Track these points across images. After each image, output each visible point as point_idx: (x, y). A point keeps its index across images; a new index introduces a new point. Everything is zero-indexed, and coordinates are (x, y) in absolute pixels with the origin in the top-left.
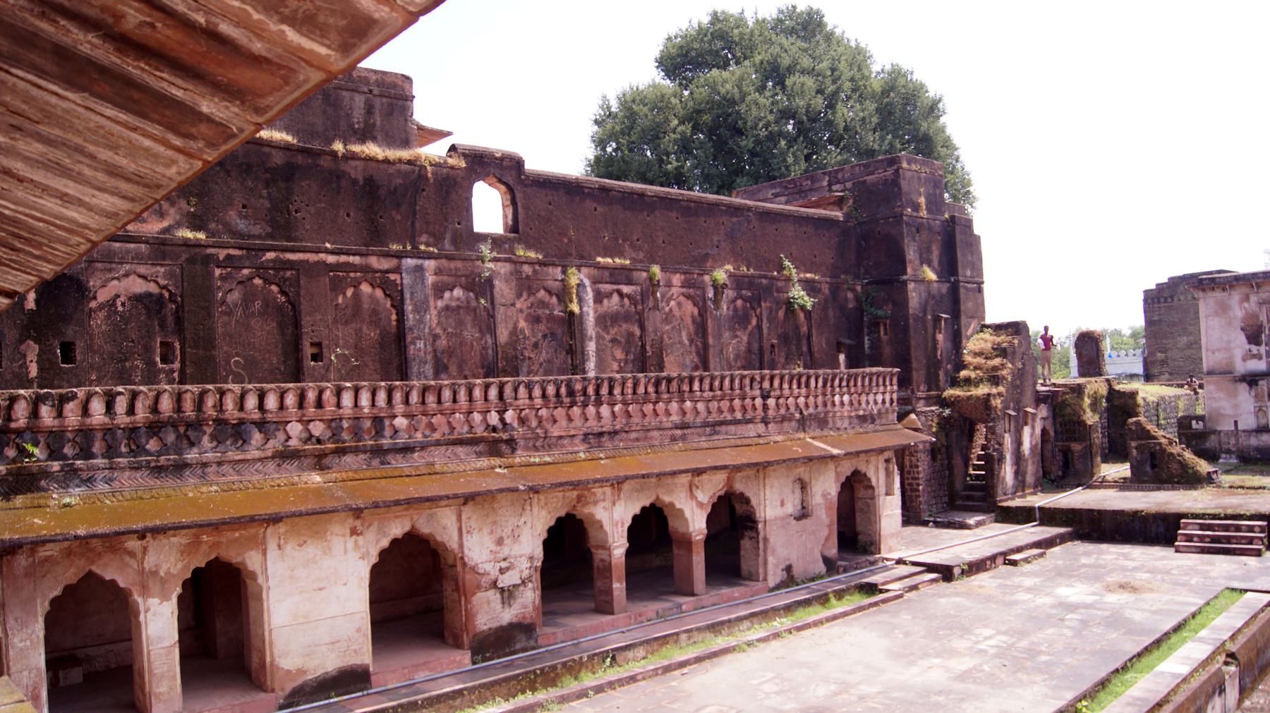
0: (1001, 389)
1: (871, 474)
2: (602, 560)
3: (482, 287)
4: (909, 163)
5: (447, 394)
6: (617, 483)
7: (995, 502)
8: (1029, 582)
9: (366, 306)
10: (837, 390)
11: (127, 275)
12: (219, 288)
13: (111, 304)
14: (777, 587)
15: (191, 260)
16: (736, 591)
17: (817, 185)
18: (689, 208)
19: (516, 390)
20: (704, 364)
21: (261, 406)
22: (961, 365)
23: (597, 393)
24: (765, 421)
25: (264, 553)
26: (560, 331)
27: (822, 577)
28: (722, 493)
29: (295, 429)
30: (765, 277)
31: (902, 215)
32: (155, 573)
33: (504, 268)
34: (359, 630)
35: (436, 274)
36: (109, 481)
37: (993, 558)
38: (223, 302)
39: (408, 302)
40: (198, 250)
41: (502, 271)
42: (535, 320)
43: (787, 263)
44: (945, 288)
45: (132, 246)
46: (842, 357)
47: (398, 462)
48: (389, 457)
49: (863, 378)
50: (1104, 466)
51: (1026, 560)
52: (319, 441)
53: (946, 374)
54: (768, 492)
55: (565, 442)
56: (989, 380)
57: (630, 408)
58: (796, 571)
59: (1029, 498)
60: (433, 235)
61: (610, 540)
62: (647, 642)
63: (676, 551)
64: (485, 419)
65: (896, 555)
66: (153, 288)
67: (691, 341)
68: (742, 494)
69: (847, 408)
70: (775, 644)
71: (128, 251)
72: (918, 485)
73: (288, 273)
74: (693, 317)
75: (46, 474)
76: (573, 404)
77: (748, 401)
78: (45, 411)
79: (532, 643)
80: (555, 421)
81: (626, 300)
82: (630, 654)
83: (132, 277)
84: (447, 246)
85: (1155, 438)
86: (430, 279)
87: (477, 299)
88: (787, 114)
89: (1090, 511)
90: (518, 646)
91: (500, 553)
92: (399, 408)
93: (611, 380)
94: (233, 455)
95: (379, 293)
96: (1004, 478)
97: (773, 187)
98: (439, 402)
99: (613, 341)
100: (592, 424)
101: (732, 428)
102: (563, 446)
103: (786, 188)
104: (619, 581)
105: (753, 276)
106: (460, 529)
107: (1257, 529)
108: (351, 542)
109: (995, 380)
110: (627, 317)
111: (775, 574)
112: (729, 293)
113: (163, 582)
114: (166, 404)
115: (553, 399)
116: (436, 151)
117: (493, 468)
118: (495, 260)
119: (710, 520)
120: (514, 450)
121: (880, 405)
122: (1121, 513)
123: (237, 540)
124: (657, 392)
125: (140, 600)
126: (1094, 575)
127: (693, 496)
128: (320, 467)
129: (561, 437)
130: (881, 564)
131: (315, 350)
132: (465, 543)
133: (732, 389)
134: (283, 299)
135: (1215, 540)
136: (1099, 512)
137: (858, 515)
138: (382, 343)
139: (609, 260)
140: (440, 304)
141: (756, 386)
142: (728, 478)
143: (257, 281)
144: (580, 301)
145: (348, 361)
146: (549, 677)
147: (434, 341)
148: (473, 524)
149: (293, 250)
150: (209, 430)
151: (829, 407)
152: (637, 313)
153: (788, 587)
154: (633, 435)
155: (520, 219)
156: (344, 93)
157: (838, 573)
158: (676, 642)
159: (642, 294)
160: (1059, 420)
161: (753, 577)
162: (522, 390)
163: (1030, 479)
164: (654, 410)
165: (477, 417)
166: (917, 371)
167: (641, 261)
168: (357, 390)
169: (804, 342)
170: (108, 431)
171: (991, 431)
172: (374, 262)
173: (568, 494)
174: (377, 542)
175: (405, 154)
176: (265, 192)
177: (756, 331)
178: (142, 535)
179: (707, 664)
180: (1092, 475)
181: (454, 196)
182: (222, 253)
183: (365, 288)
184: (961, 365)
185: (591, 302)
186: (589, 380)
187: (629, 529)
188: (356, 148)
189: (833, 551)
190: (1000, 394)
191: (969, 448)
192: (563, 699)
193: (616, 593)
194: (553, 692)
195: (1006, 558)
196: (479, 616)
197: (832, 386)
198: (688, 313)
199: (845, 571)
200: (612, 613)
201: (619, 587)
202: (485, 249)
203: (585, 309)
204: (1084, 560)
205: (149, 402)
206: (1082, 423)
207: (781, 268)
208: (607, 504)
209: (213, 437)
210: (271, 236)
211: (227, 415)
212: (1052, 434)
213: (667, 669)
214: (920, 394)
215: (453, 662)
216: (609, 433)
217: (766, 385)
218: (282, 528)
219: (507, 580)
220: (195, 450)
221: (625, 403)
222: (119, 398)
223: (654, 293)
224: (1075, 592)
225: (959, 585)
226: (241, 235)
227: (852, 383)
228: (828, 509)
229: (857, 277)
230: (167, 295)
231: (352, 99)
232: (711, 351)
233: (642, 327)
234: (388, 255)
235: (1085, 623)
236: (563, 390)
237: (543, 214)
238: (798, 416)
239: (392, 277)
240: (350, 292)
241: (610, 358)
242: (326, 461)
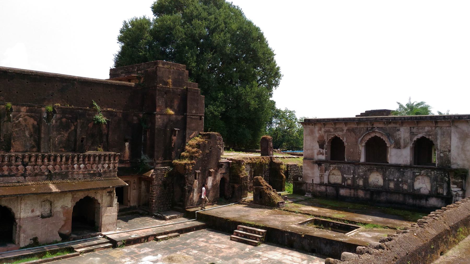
1: (98, 197)
4: (164, 64)
17: (133, 70)
20: (38, 146)
22: (183, 150)
24: (24, 175)
30: (81, 109)
31: (156, 86)
44: (180, 118)
46: (127, 144)
54: (23, 206)
58: (40, 240)
59: (207, 208)
67: (31, 136)
72: (153, 199)
74: (34, 126)
85: (262, 186)
88: (192, 37)
96: (192, 199)
103: (125, 70)
107: (261, 233)
109: (191, 158)
111: (25, 241)
121: (106, 169)
135: (245, 236)
151: (70, 170)
153: (34, 247)
157: (70, 241)
180: (241, 198)
189: (67, 231)
190: (192, 164)
197: (73, 161)
212: (228, 179)
217: (26, 160)
223: (8, 115)
227: (87, 159)
232: (42, 140)
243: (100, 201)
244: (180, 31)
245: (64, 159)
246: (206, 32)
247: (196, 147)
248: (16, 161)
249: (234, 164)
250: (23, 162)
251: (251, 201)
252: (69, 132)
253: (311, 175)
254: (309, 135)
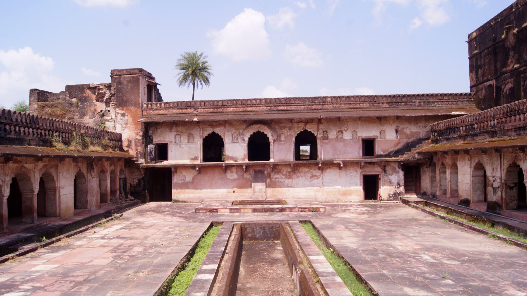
11: (508, 83)
13: (506, 92)
47: (475, 138)
100: (518, 124)
128: (464, 140)
129: (508, 130)
219: (496, 185)
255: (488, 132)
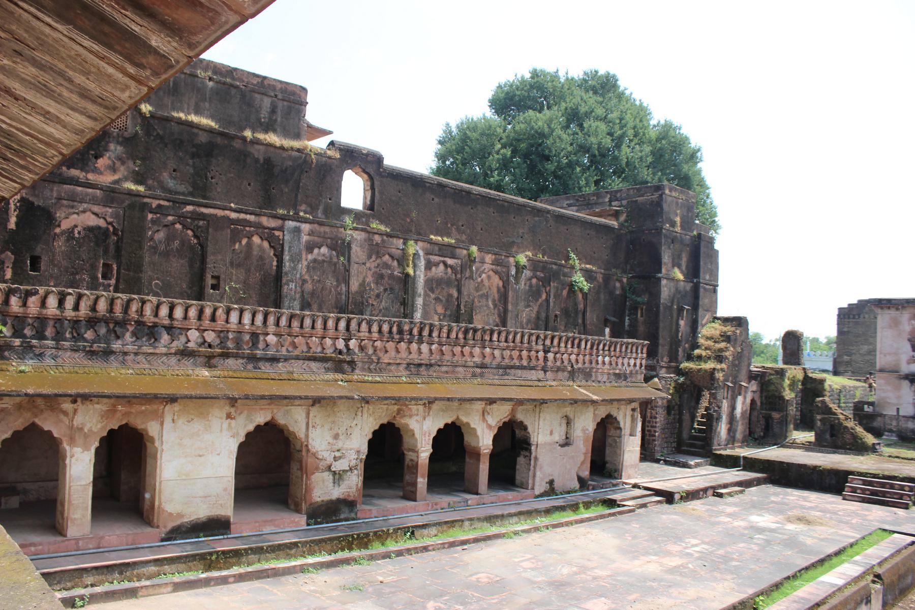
0: (724, 366)
1: (620, 418)
2: (412, 460)
3: (342, 247)
4: (670, 191)
5: (308, 322)
6: (430, 403)
7: (711, 450)
8: (729, 510)
9: (255, 253)
10: (601, 352)
11: (84, 212)
12: (150, 228)
14: (541, 495)
15: (132, 206)
16: (510, 495)
18: (503, 206)
19: (359, 325)
20: (504, 323)
21: (171, 315)
22: (695, 346)
23: (420, 334)
25: (162, 424)
26: (397, 287)
27: (575, 492)
28: (507, 420)
29: (194, 335)
31: (662, 228)
32: (81, 429)
33: (359, 236)
34: (225, 490)
35: (309, 235)
36: (54, 358)
37: (705, 490)
38: (152, 239)
39: (286, 253)
40: (137, 199)
41: (359, 238)
42: (379, 278)
43: (572, 255)
44: (689, 286)
45: (90, 190)
46: (607, 330)
47: (266, 368)
48: (261, 364)
49: (621, 345)
50: (795, 433)
51: (730, 494)
52: (210, 346)
53: (684, 351)
55: (393, 368)
56: (715, 359)
57: (444, 348)
58: (556, 485)
59: (737, 450)
60: (310, 206)
61: (419, 445)
62: (439, 524)
63: (467, 460)
64: (334, 344)
65: (633, 481)
66: (102, 223)
67: (495, 306)
68: (521, 422)
69: (607, 366)
70: (535, 535)
71: (87, 194)
72: (655, 432)
73: (201, 223)
74: (498, 288)
75: (9, 347)
76: (401, 340)
77: (533, 353)
78: (14, 301)
79: (353, 515)
80: (386, 352)
81: (449, 270)
82: (425, 531)
83: (88, 213)
84: (320, 215)
85: (835, 414)
86: (305, 238)
87: (338, 256)
88: (584, 149)
89: (782, 463)
90: (342, 516)
91: (336, 447)
92: (271, 328)
93: (431, 325)
94: (146, 349)
95: (266, 244)
96: (719, 433)
97: (568, 199)
98: (301, 327)
99: (437, 299)
101: (519, 371)
102: (390, 371)
103: (577, 200)
104: (423, 477)
105: (546, 262)
106: (308, 424)
108: (226, 423)
109: (720, 359)
110: (449, 283)
111: (540, 485)
112: (527, 273)
113: (86, 436)
114: (102, 306)
115: (387, 335)
116: (320, 144)
117: (336, 381)
118: (355, 229)
119: (496, 439)
120: (353, 370)
121: (632, 368)
122: (805, 466)
123: (142, 412)
124: (465, 338)
125: (68, 448)
126: (778, 510)
127: (484, 420)
128: (210, 366)
129: (389, 364)
130: (621, 487)
131: (214, 282)
132: (310, 434)
133: (522, 342)
134: (195, 241)
136: (788, 464)
137: (607, 448)
138: (263, 283)
139: (440, 238)
140: (310, 257)
141: (540, 342)
142: (513, 410)
143: (178, 226)
144: (415, 266)
145: (238, 292)
146: (363, 541)
147: (303, 284)
148: (318, 421)
149: (206, 206)
150: (131, 329)
151: (594, 365)
152: (457, 280)
154: (444, 369)
155: (376, 201)
156: (256, 95)
157: (588, 490)
158: (461, 526)
159: (462, 266)
160: (764, 394)
161: (524, 486)
162: (364, 325)
163: (739, 436)
164: (462, 352)
165: (328, 342)
166: (663, 346)
167: (463, 242)
168: (242, 312)
169: (580, 316)
170: (58, 321)
171: (714, 396)
172: (265, 221)
173: (390, 407)
174: (245, 426)
175: (296, 144)
176: (191, 162)
177: (545, 304)
178: (74, 399)
179: (482, 544)
180: (786, 437)
181: (328, 179)
182: (155, 203)
183: (256, 240)
184: (695, 346)
185: (423, 268)
186: (415, 324)
187: (434, 439)
188: (261, 136)
189: (586, 473)
190: (722, 370)
191: (696, 408)
192: (372, 558)
193: (419, 486)
194: (364, 552)
195: (715, 491)
196: (315, 490)
197: (597, 349)
198: (495, 284)
199: (593, 489)
200: (415, 500)
201: (422, 482)
202: (348, 220)
203: (418, 273)
204: (773, 498)
205: (90, 303)
206: (781, 398)
207: (568, 258)
208: (419, 418)
209: (134, 334)
210: (191, 194)
211: (145, 319)
212: (759, 403)
213: (452, 545)
214: (663, 364)
215: (293, 522)
216: (426, 365)
217: (548, 342)
218: (176, 407)
219: (338, 466)
220: (120, 342)
221: (440, 344)
222: (68, 298)
223: (471, 267)
224: (764, 520)
225: (678, 507)
226: (170, 191)
227: (612, 349)
228: (585, 441)
229: (624, 271)
230: (111, 229)
231: (262, 100)
232: (510, 315)
233: (459, 291)
234: (275, 217)
235: (768, 542)
236: (395, 329)
237: (394, 198)
238: (569, 368)
239: (277, 233)
240: (244, 241)
241: (432, 312)
242: (214, 361)
243: (622, 425)
244: (562, 141)
245: (589, 346)
246: (608, 142)
247: (723, 341)
248: (536, 344)
249: (771, 374)
250: (544, 344)
251: (810, 442)
252: (539, 303)
253: (894, 401)
254: (890, 327)
255: (324, 360)
